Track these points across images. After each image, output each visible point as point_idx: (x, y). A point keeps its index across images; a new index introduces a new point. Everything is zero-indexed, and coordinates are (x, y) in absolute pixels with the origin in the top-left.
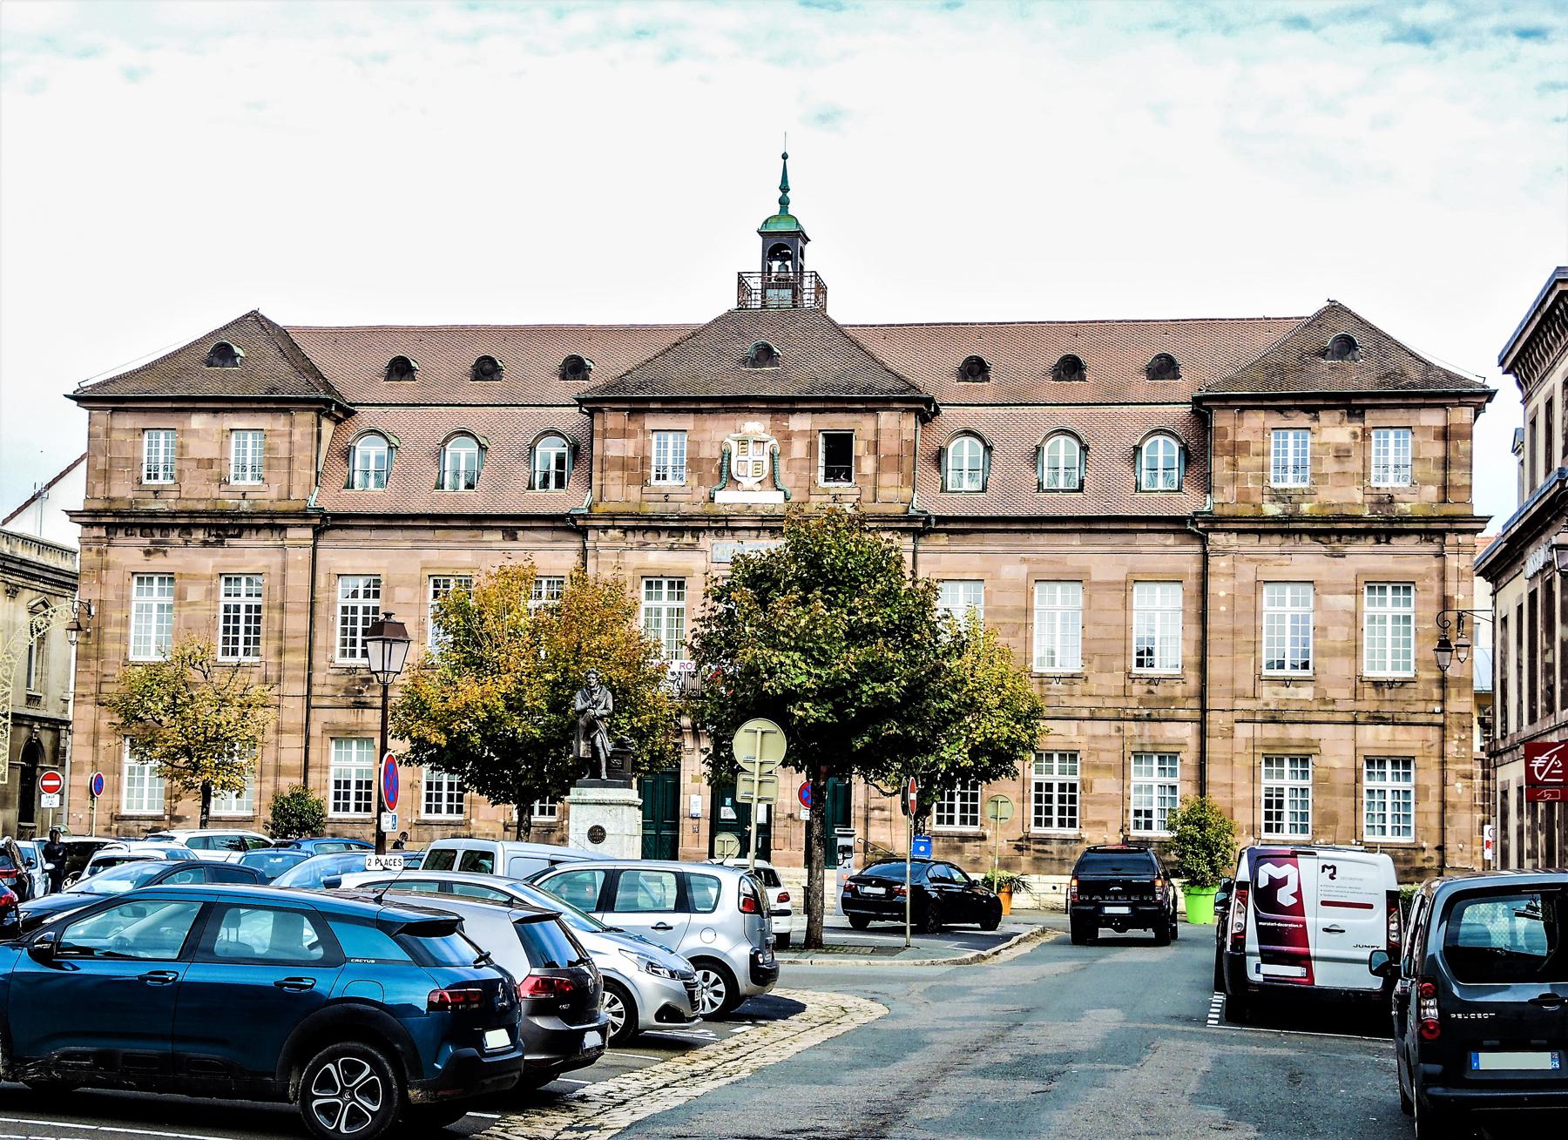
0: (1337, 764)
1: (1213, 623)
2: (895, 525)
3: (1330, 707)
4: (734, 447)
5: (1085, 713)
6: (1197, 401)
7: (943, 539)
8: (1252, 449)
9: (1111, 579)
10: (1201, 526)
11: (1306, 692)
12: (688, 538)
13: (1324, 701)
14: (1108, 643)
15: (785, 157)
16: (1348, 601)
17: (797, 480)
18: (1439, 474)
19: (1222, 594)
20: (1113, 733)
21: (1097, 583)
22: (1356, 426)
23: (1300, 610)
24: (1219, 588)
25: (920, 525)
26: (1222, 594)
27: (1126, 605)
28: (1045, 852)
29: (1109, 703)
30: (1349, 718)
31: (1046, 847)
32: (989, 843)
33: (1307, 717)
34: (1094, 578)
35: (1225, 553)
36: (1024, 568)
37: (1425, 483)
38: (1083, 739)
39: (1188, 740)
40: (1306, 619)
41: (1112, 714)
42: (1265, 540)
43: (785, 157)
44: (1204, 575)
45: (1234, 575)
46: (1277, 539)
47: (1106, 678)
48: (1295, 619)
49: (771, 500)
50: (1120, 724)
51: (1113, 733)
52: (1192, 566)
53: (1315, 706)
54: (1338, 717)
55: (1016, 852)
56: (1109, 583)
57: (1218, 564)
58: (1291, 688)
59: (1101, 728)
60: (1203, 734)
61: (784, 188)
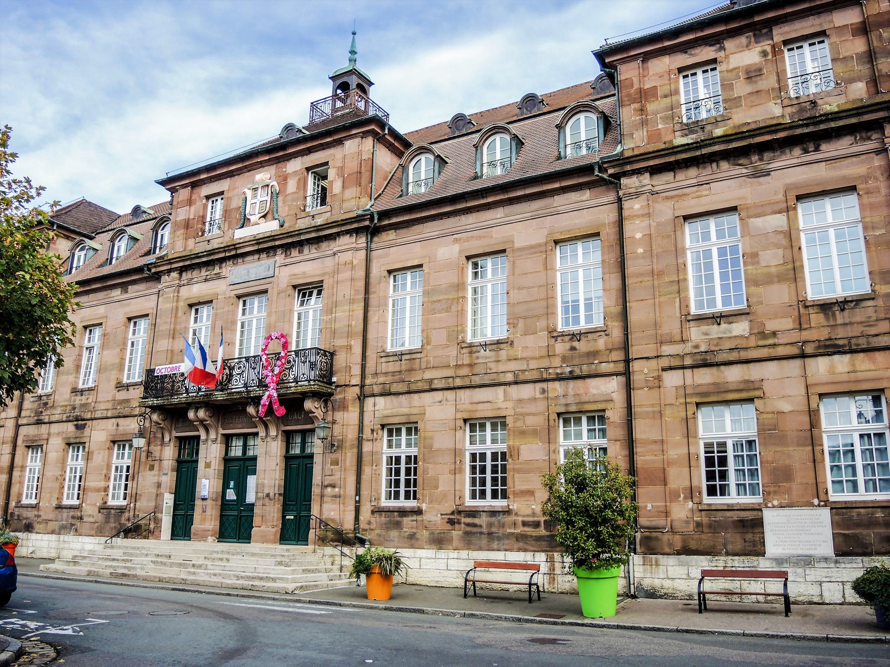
0: (786, 407)
1: (631, 268)
2: (348, 227)
3: (771, 341)
4: (249, 194)
5: (510, 377)
6: (600, 56)
7: (391, 235)
8: (660, 92)
9: (533, 242)
10: (611, 171)
11: (741, 328)
12: (217, 270)
13: (762, 335)
14: (531, 308)
15: (354, 34)
16: (779, 221)
17: (289, 210)
18: (865, 69)
19: (638, 236)
20: (538, 395)
21: (521, 249)
22: (766, 45)
23: (727, 242)
24: (635, 231)
25: (367, 223)
26: (638, 236)
27: (548, 266)
28: (475, 525)
29: (533, 365)
30: (795, 351)
31: (476, 521)
32: (426, 517)
33: (744, 355)
34: (517, 245)
35: (638, 194)
36: (456, 248)
37: (852, 81)
38: (509, 405)
39: (615, 396)
40: (734, 249)
41: (535, 375)
42: (681, 175)
43: (354, 34)
44: (620, 223)
45: (649, 215)
46: (693, 172)
47: (530, 340)
48: (722, 252)
49: (271, 227)
50: (544, 385)
51: (538, 395)
52: (608, 215)
53: (752, 342)
54: (781, 351)
55: (449, 527)
56: (531, 247)
57: (633, 206)
58: (723, 326)
59: (527, 391)
60: (629, 388)
61: (353, 52)
